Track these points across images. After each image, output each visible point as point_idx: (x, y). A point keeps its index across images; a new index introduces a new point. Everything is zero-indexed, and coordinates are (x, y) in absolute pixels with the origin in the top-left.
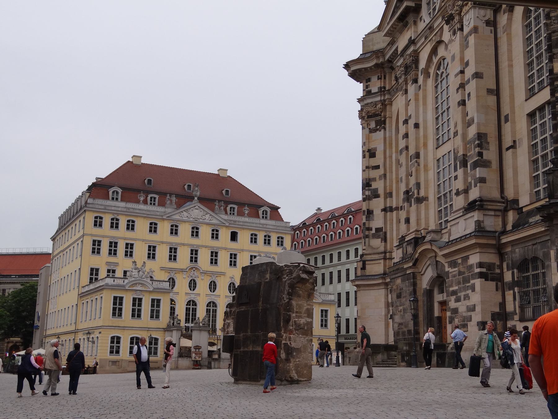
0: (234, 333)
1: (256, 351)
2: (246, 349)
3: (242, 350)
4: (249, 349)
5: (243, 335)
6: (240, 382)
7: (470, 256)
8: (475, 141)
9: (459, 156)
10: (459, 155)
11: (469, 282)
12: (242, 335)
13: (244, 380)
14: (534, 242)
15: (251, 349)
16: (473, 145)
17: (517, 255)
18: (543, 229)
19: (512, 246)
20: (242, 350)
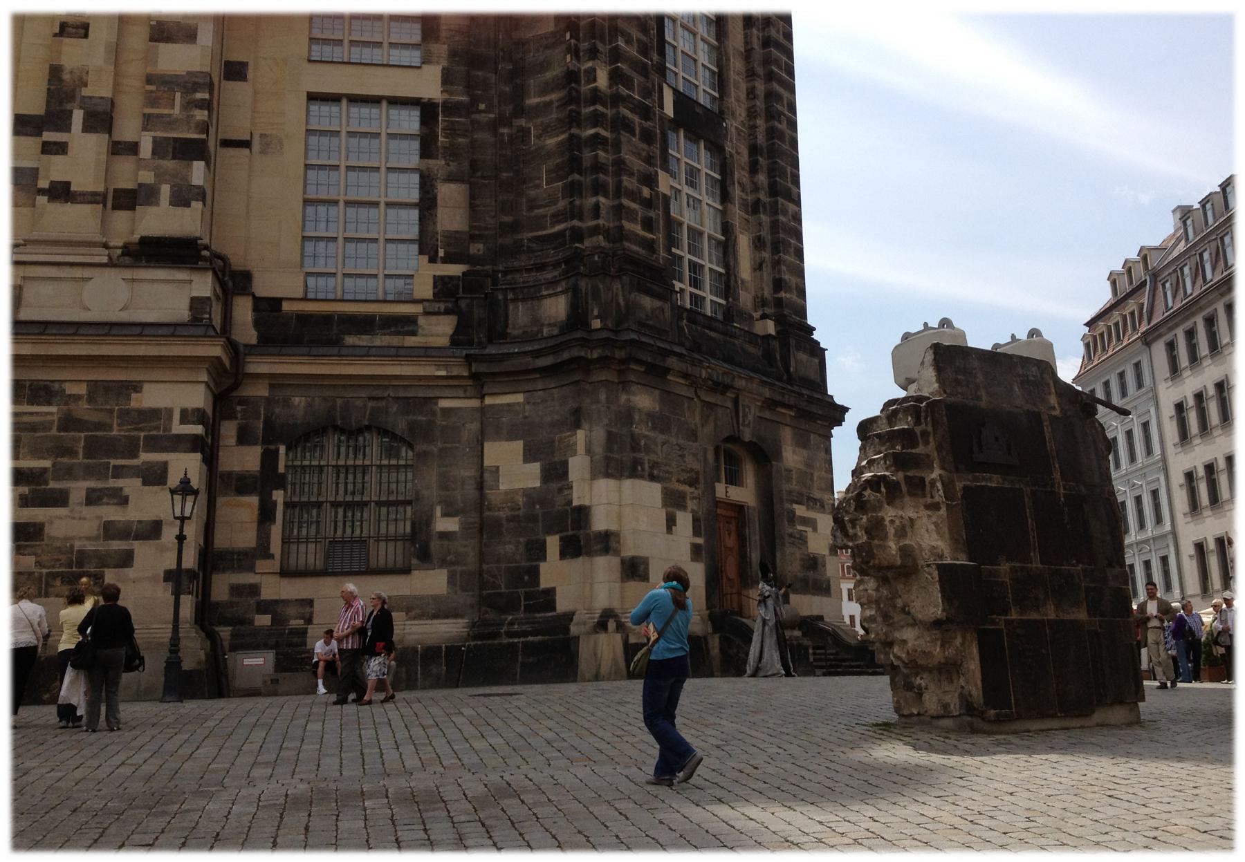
0: (963, 556)
1: (1074, 622)
2: (1034, 616)
3: (1014, 615)
4: (1047, 615)
5: (1013, 569)
6: (1017, 725)
7: (146, 387)
8: (195, 91)
9: (90, 98)
10: (85, 92)
11: (136, 456)
12: (1005, 567)
13: (1044, 715)
14: (379, 393)
15: (1052, 616)
16: (178, 95)
17: (300, 413)
18: (443, 373)
19: (272, 386)
20: (1014, 615)
